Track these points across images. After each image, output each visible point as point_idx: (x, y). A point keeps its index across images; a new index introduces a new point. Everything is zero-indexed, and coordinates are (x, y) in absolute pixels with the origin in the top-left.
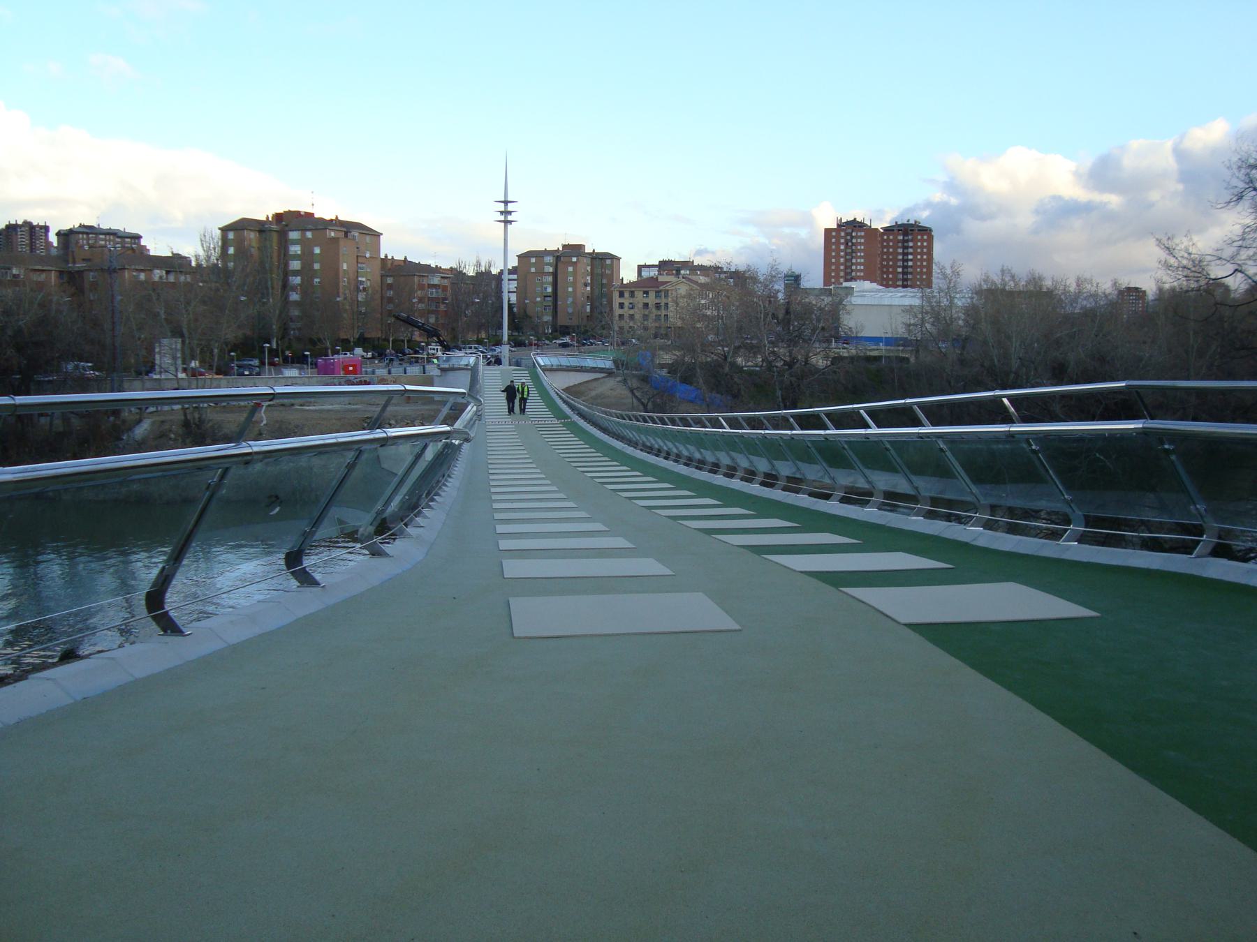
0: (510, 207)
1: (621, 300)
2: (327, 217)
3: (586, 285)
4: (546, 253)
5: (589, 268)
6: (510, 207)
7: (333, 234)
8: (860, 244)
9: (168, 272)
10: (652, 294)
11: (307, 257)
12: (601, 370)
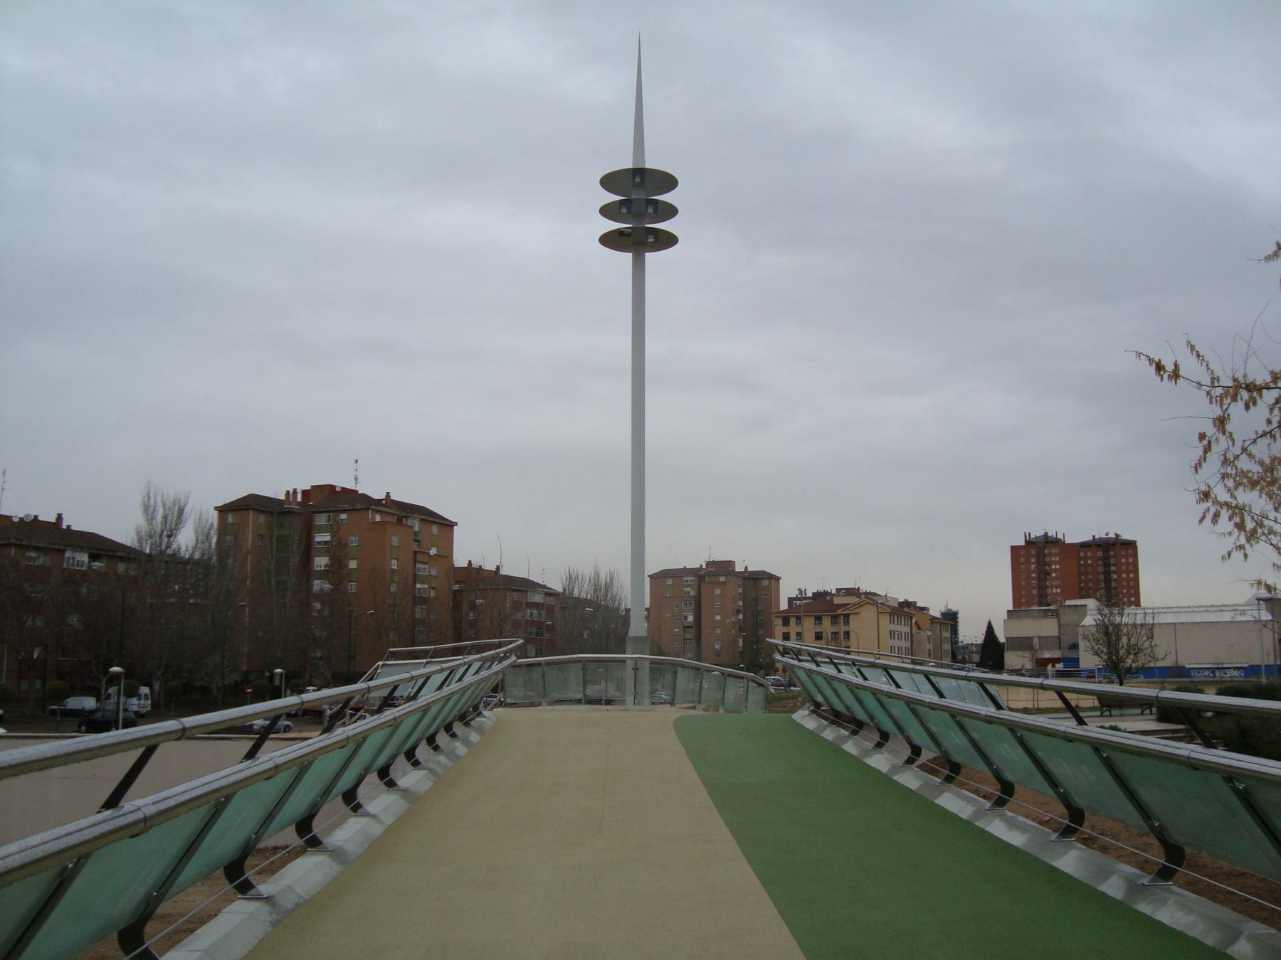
1: (785, 630)
2: (376, 497)
3: (738, 612)
4: (685, 571)
5: (740, 590)
7: (378, 518)
8: (1055, 563)
9: (93, 557)
10: (827, 621)
11: (337, 552)
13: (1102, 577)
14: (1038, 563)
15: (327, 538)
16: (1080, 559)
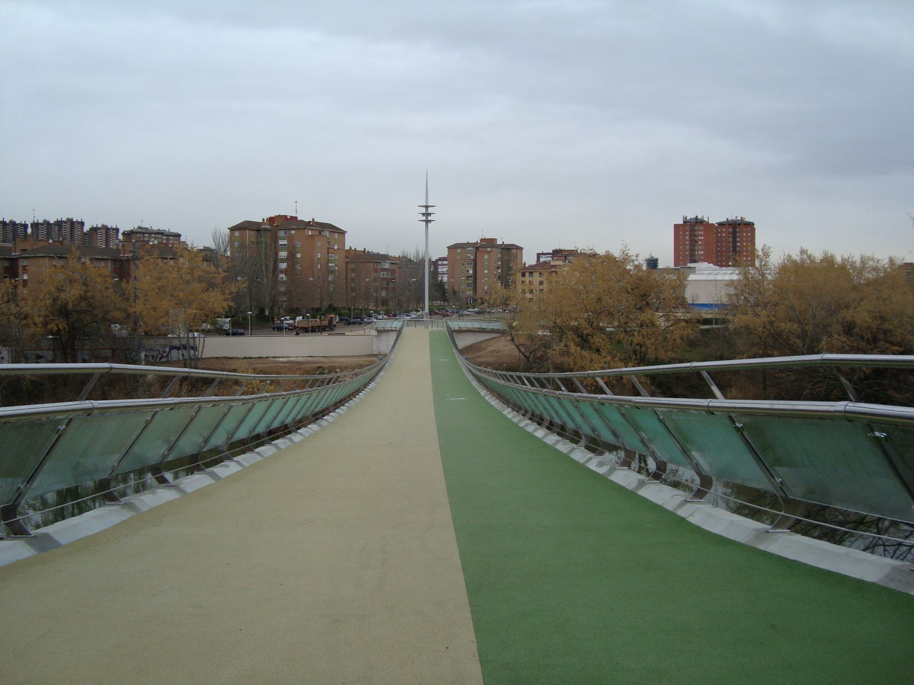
0: (430, 210)
1: (523, 279)
4: (468, 245)
6: (430, 210)
8: (701, 235)
12: (497, 331)
13: (731, 244)
14: (690, 235)
15: (285, 242)
16: (718, 232)
